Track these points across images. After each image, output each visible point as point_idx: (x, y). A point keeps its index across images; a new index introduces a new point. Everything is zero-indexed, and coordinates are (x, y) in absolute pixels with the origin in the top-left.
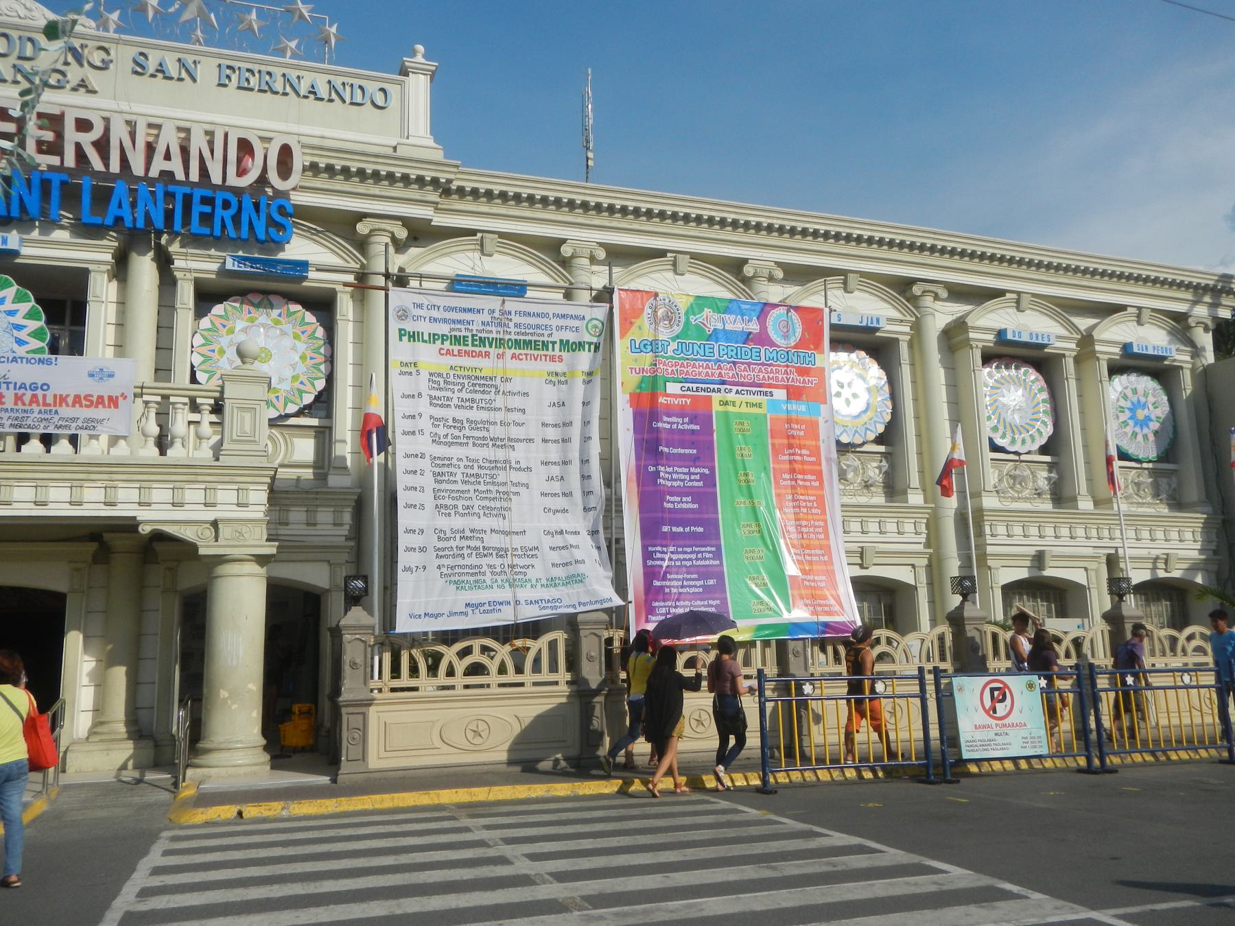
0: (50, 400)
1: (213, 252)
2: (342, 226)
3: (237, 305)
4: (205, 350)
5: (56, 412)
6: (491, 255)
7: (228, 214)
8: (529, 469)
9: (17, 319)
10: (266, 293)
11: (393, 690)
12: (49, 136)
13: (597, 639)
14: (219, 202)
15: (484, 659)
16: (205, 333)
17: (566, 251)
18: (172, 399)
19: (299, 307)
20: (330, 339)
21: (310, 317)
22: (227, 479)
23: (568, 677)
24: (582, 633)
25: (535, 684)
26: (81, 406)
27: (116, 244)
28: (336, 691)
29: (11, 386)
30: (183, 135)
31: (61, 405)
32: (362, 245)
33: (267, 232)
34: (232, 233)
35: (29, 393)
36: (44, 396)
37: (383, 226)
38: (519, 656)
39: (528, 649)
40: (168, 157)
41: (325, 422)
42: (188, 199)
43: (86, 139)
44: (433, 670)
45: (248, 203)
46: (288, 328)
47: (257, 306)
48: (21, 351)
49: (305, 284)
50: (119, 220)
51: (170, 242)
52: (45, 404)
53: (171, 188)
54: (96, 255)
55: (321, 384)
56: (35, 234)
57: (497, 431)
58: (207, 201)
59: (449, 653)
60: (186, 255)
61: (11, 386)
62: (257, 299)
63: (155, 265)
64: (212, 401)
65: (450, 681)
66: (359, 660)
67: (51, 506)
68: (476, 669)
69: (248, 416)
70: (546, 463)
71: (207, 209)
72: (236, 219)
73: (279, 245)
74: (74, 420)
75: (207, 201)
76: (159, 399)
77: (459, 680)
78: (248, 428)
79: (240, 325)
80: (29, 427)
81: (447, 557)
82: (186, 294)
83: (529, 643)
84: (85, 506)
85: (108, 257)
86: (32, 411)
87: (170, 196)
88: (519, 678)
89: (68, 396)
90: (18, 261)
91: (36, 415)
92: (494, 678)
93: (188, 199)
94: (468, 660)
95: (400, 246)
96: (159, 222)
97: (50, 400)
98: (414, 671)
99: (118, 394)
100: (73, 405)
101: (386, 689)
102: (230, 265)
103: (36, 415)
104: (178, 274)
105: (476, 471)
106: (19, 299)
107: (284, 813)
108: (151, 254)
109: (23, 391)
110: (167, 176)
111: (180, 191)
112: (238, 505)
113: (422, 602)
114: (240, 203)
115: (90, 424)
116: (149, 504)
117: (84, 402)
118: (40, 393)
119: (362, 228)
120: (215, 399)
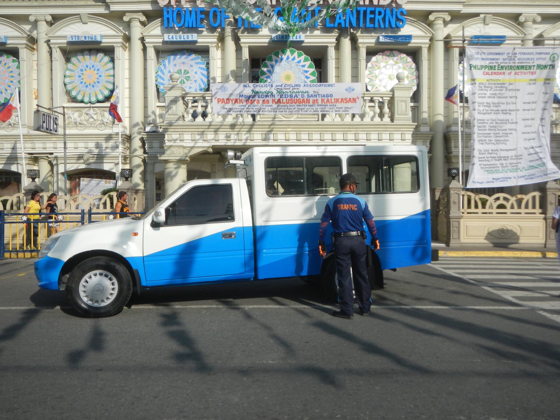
0: (333, 101)
1: (373, 34)
2: (424, 17)
3: (381, 56)
4: (369, 76)
6: (488, 25)
8: (516, 123)
9: (306, 68)
10: (391, 50)
11: (468, 213)
13: (554, 196)
14: (377, 13)
15: (504, 203)
16: (370, 69)
17: (522, 19)
18: (375, 98)
19: (405, 55)
20: (418, 68)
21: (409, 59)
22: (397, 129)
23: (540, 211)
24: (548, 193)
25: (526, 213)
28: (448, 212)
32: (430, 24)
33: (396, 24)
35: (326, 98)
37: (440, 16)
38: (519, 202)
39: (523, 199)
41: (416, 104)
42: (365, 12)
44: (484, 206)
45: (388, 12)
46: (401, 65)
47: (389, 56)
48: (308, 81)
49: (409, 45)
50: (340, 24)
51: (357, 32)
52: (332, 103)
53: (359, 9)
54: (329, 40)
55: (415, 88)
56: (308, 33)
57: (503, 107)
58: (373, 12)
59: (491, 200)
60: (363, 36)
62: (388, 53)
63: (350, 42)
64: (389, 98)
65: (490, 211)
66: (456, 201)
67: (337, 141)
68: (501, 206)
69: (403, 104)
70: (524, 120)
71: (372, 16)
72: (384, 19)
73: (398, 28)
74: (341, 108)
75: (373, 12)
77: (495, 210)
78: (404, 109)
79: (382, 64)
81: (483, 161)
82: (363, 52)
83: (523, 196)
84: (348, 141)
85: (334, 40)
86: (327, 105)
87: (358, 12)
88: (519, 211)
90: (303, 45)
92: (508, 210)
93: (365, 12)
94: (499, 202)
95: (446, 23)
96: (354, 24)
97: (333, 101)
98: (476, 207)
101: (465, 213)
102: (382, 39)
104: (360, 45)
105: (494, 124)
106: (306, 60)
107: (445, 255)
108: (349, 37)
111: (362, 9)
112: (402, 140)
113: (479, 178)
114: (385, 11)
115: (346, 110)
116: (370, 140)
118: (329, 98)
119: (431, 17)
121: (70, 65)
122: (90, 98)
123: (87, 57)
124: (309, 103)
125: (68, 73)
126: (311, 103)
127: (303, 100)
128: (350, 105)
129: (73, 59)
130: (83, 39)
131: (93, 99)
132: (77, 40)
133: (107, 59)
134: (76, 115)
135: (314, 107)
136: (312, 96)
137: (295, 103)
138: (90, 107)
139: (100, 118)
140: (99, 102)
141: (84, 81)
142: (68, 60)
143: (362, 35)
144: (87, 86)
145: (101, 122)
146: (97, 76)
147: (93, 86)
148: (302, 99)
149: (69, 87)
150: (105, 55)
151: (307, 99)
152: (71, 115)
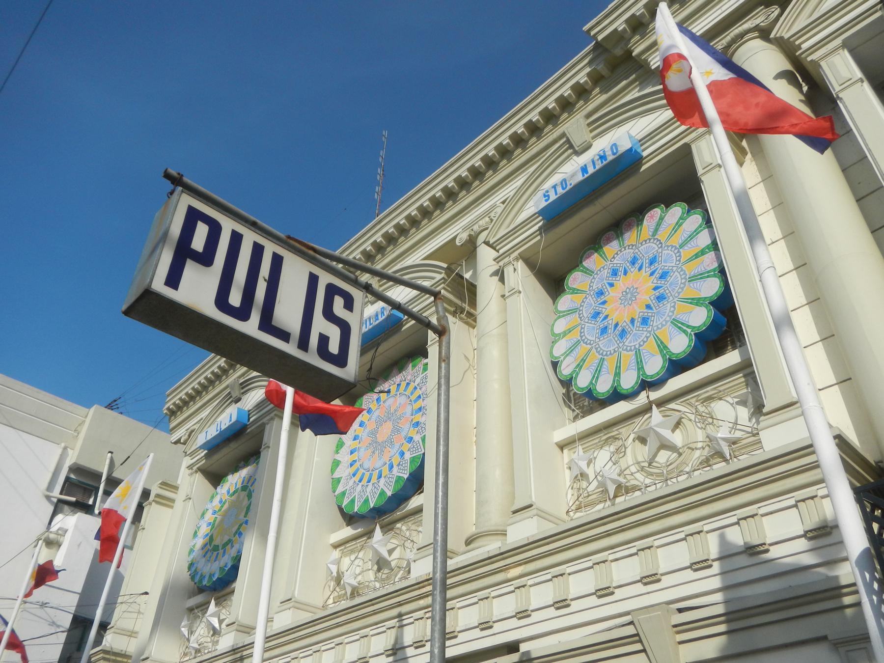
121: (565, 301)
122: (640, 368)
123: (611, 248)
125: (561, 326)
129: (575, 279)
130: (580, 177)
131: (654, 366)
132: (560, 191)
133: (677, 210)
134: (603, 456)
138: (646, 410)
139: (700, 435)
140: (677, 366)
141: (611, 322)
142: (554, 282)
144: (623, 334)
145: (706, 452)
146: (651, 283)
147: (645, 321)
149: (566, 370)
150: (667, 206)
152: (583, 464)
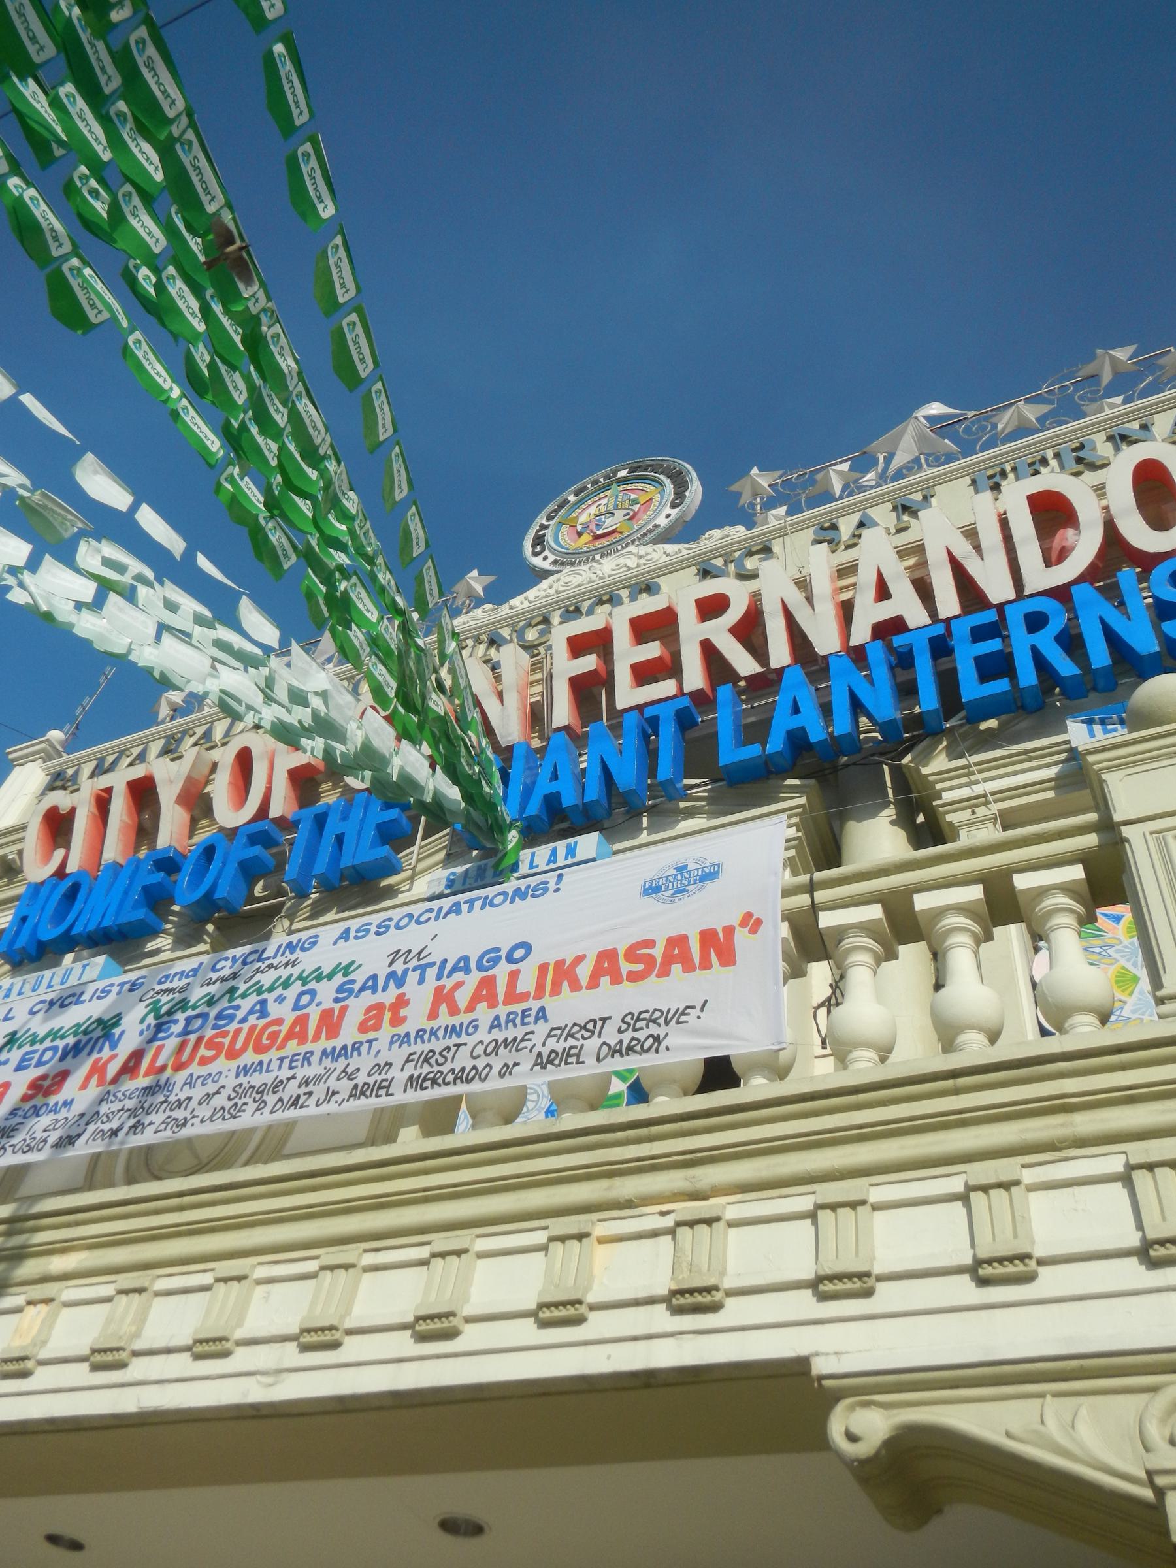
5: (542, 1014)
7: (1046, 640)
12: (652, 650)
26: (616, 980)
27: (803, 800)
29: (431, 973)
30: (911, 562)
31: (556, 991)
34: (1065, 667)
35: (476, 976)
36: (514, 976)
40: (883, 593)
43: (719, 631)
50: (798, 740)
51: (926, 758)
52: (513, 996)
60: (967, 771)
61: (431, 973)
74: (593, 1026)
76: (875, 912)
80: (461, 1077)
84: (598, 1324)
87: (903, 661)
89: (580, 959)
91: (483, 1035)
93: (941, 647)
97: (527, 982)
99: (735, 921)
100: (594, 983)
103: (483, 1035)
108: (890, 812)
109: (459, 976)
110: (889, 629)
117: (625, 967)
118: (502, 971)
120: (1083, 858)
124: (333, 1033)
126: (349, 1034)
127: (302, 1021)
128: (671, 990)
135: (363, 1063)
136: (371, 984)
137: (232, 1055)
143: (962, 762)
148: (290, 1018)
151: (326, 1015)
